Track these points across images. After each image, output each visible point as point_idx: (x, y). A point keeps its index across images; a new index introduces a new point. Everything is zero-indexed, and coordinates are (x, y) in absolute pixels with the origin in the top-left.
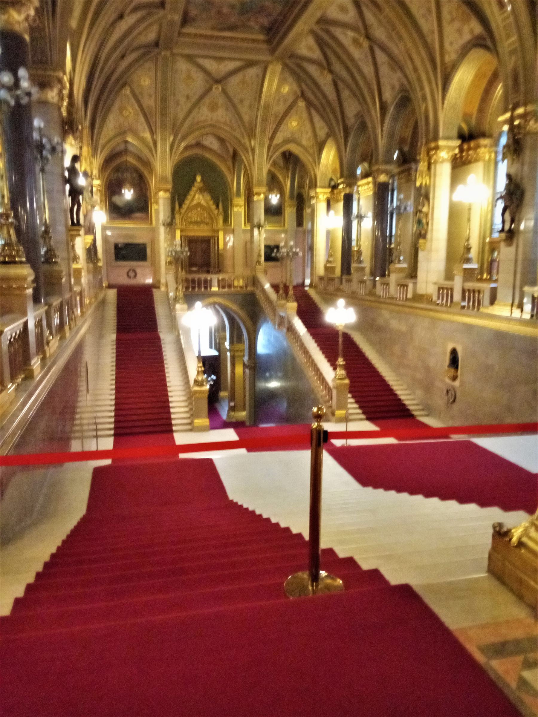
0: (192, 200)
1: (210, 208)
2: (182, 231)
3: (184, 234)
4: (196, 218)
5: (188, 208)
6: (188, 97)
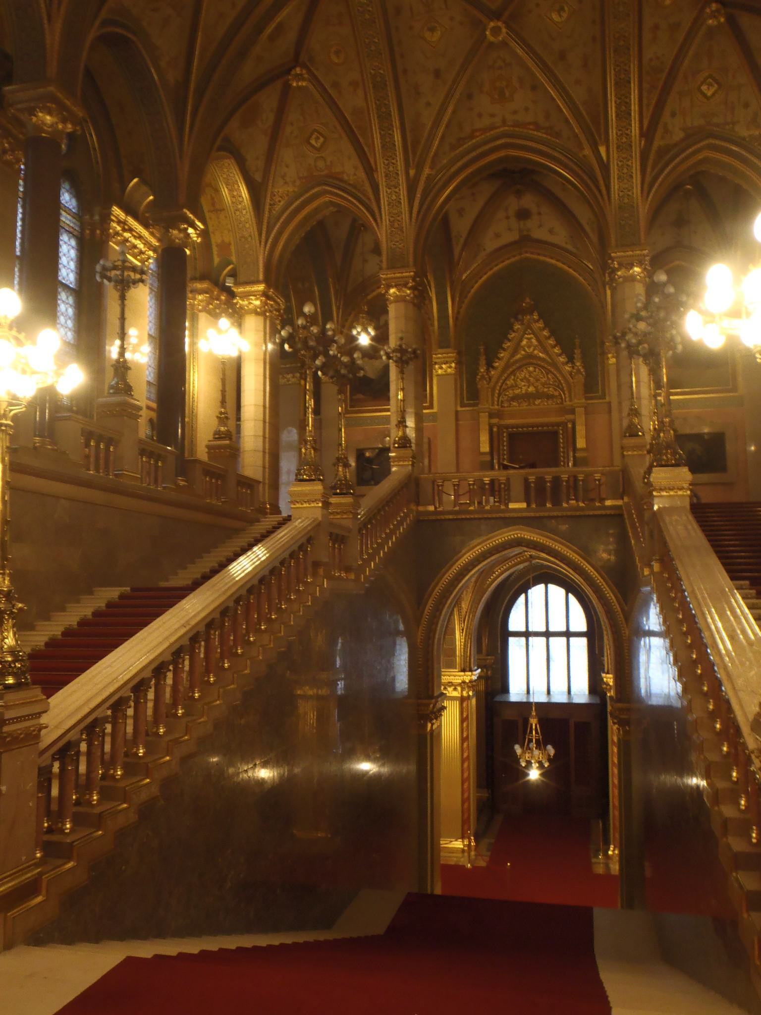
0: (515, 351)
1: (554, 364)
2: (491, 416)
3: (495, 421)
4: (524, 388)
5: (507, 366)
6: (437, 74)
